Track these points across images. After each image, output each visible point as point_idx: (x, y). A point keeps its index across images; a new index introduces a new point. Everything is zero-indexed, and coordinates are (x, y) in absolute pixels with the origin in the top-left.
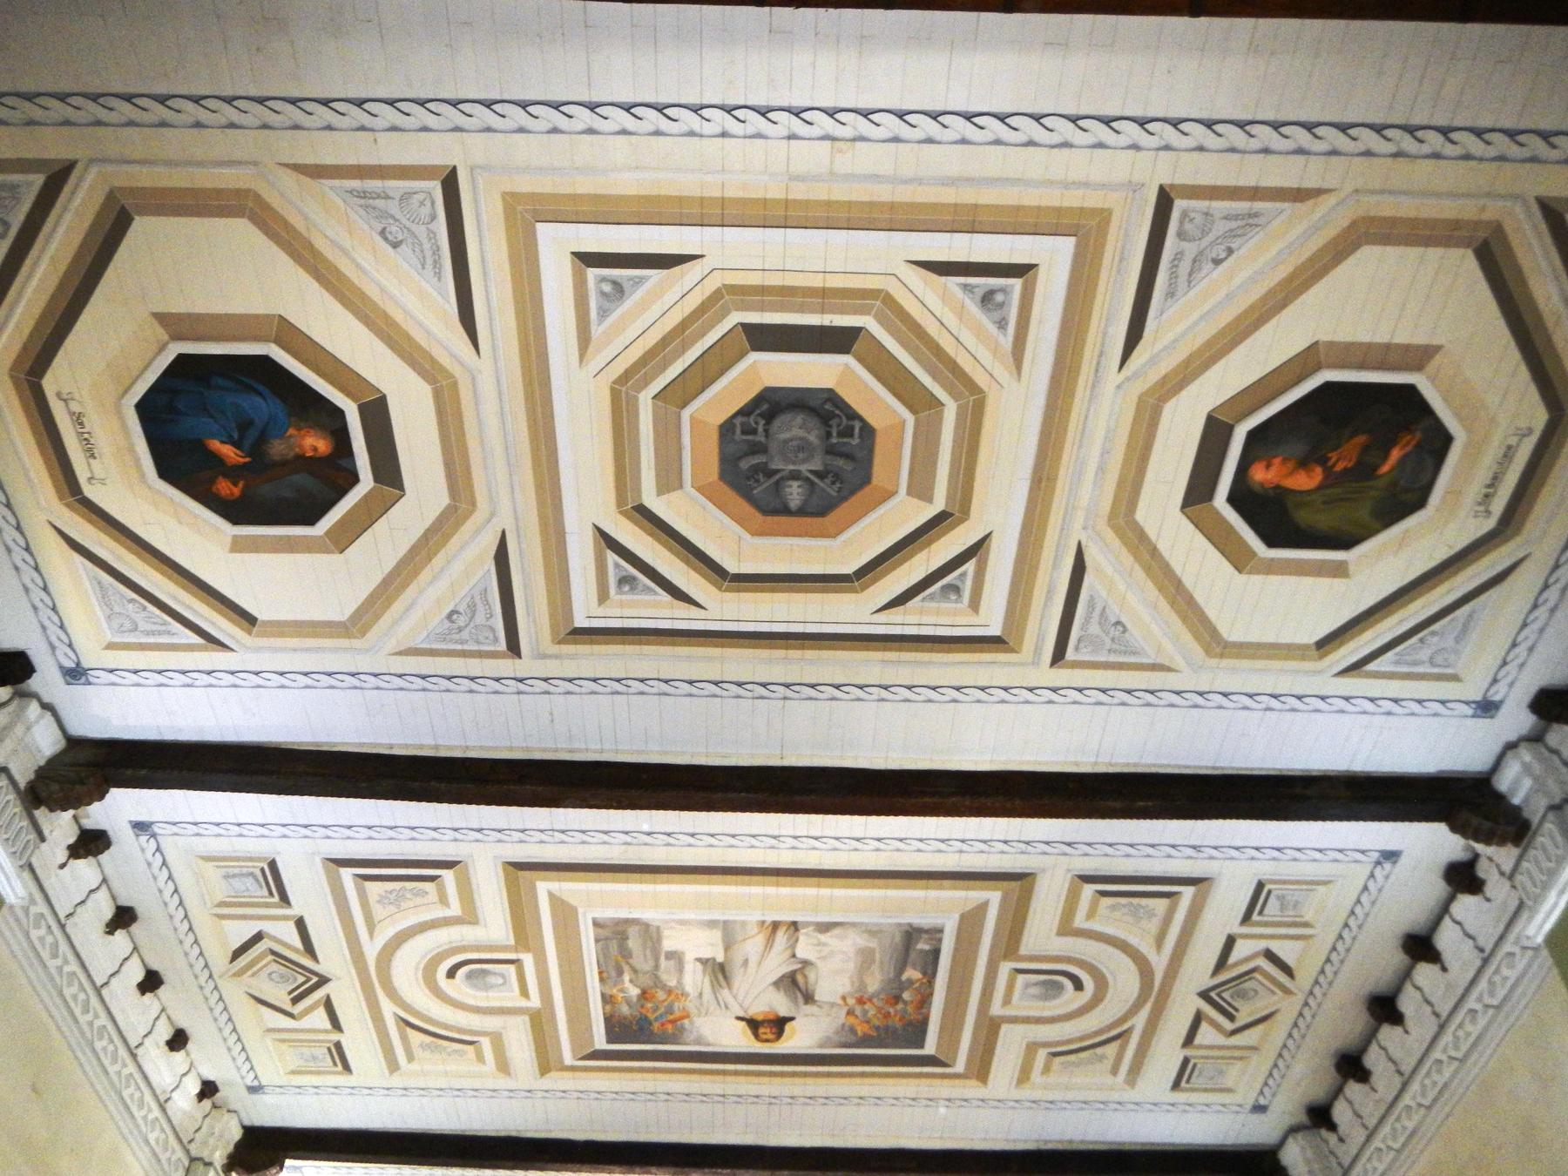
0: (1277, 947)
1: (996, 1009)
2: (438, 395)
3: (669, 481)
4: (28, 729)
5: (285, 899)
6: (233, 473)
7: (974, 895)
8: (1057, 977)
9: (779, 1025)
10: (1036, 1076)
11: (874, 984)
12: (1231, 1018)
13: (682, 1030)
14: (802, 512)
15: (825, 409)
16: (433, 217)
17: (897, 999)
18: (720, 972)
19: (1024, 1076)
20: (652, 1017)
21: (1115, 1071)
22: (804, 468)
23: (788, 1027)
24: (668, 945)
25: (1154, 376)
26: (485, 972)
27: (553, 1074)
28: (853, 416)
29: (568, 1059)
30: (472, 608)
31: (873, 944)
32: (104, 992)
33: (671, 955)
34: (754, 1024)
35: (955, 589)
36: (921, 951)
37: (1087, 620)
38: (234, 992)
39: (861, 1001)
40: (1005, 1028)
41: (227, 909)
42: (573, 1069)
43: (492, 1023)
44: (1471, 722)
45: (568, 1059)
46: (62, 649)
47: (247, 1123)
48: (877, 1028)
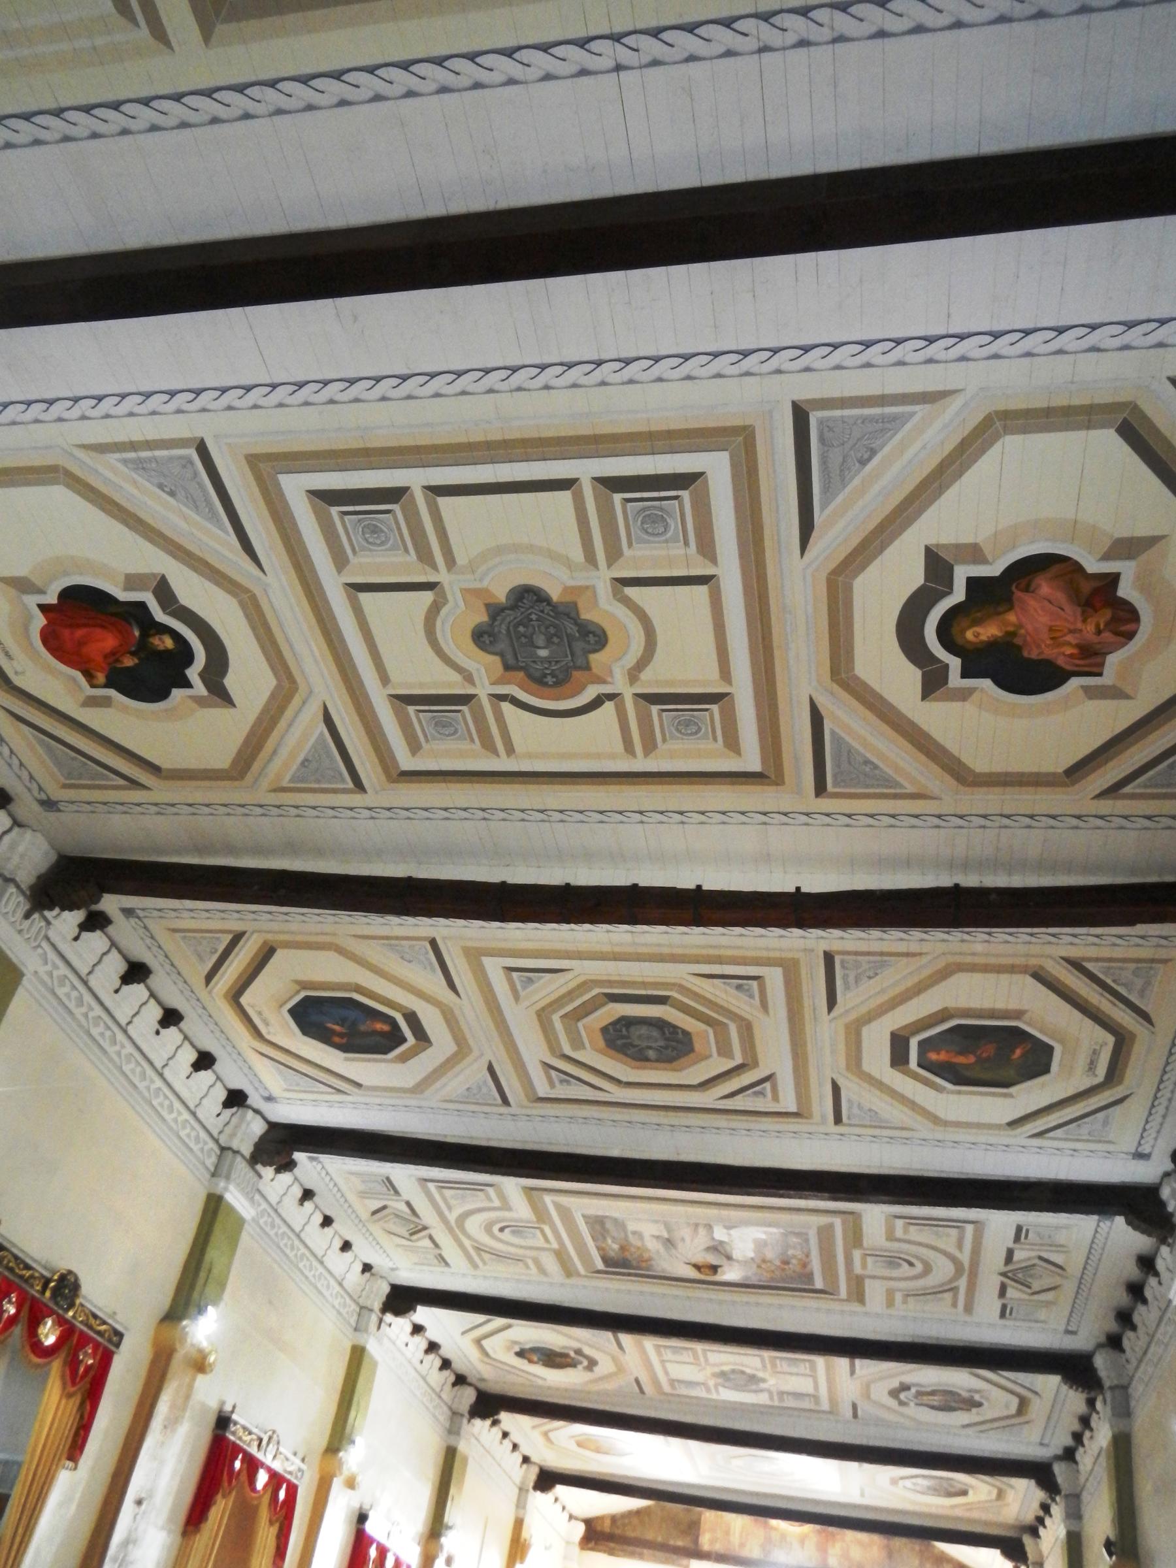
0: (1045, 1255)
1: (858, 1269)
2: (443, 1013)
4: (248, 1124)
5: (397, 1192)
6: (341, 1035)
8: (893, 1261)
9: (714, 1269)
12: (1029, 1287)
14: (657, 1061)
15: (660, 1024)
16: (427, 953)
22: (654, 1045)
25: (853, 1016)
28: (675, 1027)
30: (480, 1088)
32: (303, 1235)
33: (634, 1233)
35: (762, 1093)
37: (850, 1108)
38: (376, 1229)
41: (363, 1195)
43: (534, 1253)
44: (1135, 1162)
46: (261, 1091)
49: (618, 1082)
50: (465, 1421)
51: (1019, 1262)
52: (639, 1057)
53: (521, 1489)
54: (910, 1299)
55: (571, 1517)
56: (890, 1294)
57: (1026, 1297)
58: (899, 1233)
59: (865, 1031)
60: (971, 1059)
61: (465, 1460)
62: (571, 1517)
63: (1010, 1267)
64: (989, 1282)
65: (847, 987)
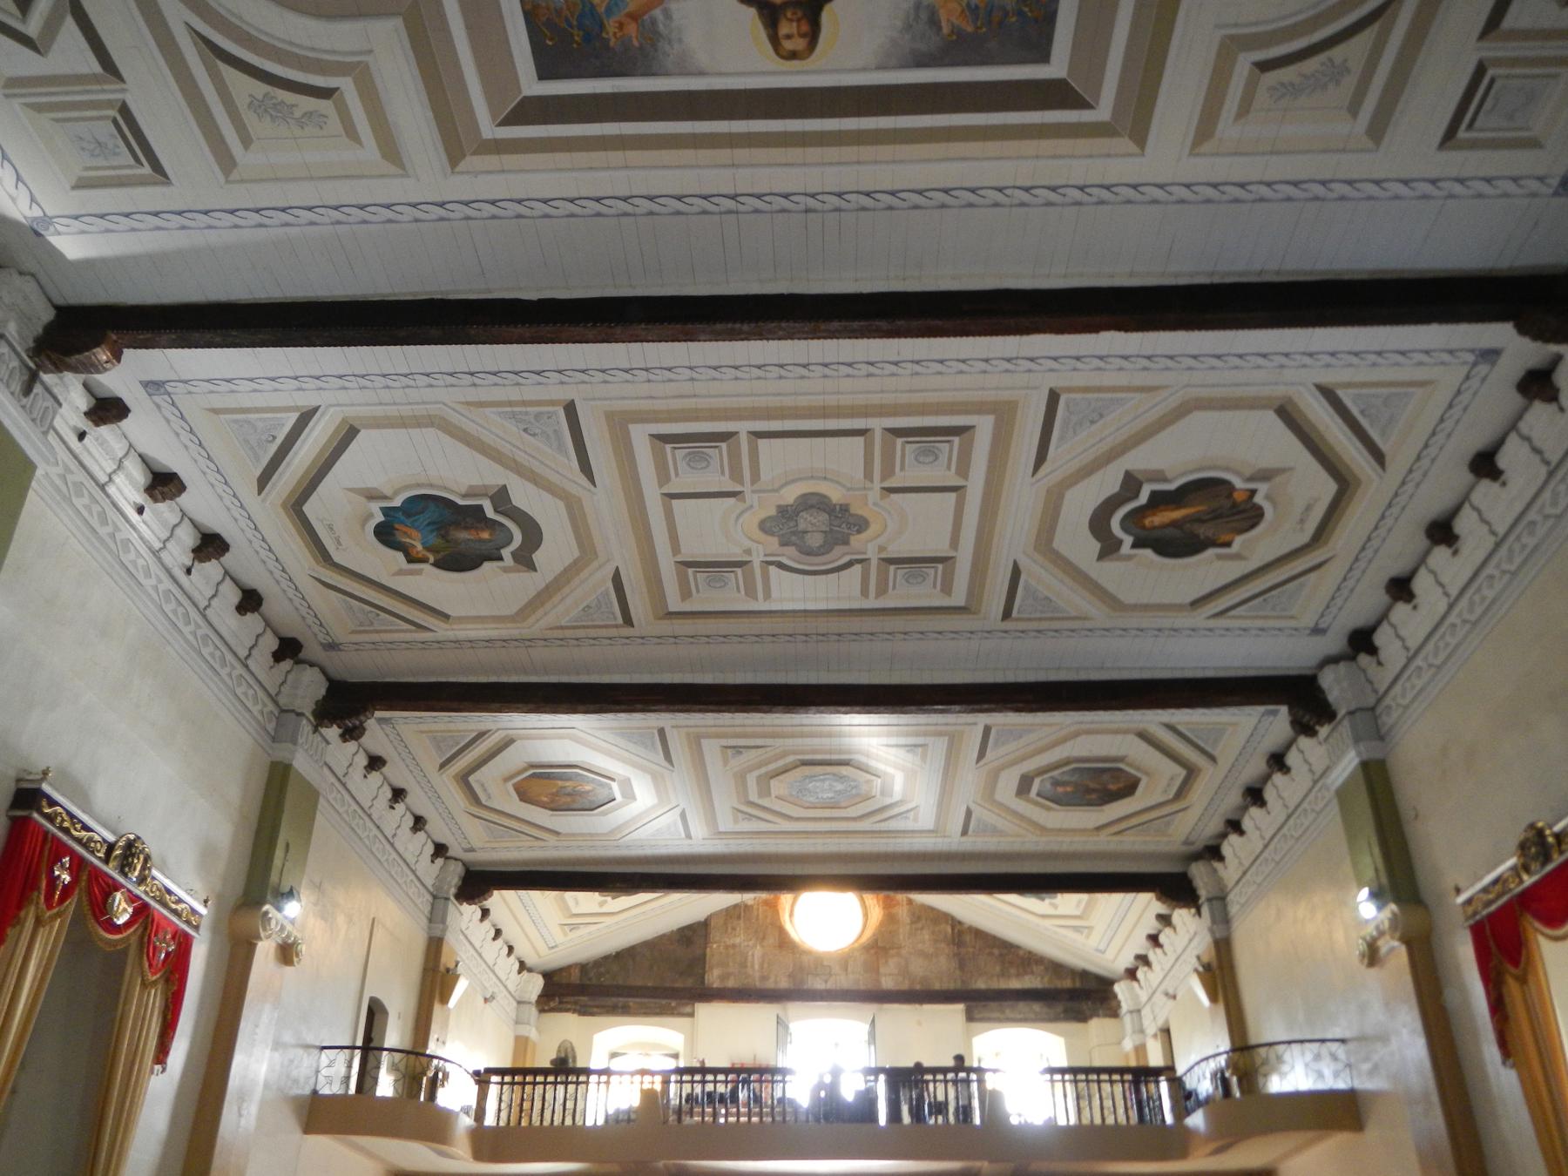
10: (1227, 128)
13: (652, 37)
19: (1205, 129)
21: (1354, 109)
27: (471, 162)
42: (499, 147)
45: (489, 129)
47: (60, 301)
50: (306, 727)
53: (435, 897)
55: (523, 967)
61: (311, 796)
62: (523, 967)
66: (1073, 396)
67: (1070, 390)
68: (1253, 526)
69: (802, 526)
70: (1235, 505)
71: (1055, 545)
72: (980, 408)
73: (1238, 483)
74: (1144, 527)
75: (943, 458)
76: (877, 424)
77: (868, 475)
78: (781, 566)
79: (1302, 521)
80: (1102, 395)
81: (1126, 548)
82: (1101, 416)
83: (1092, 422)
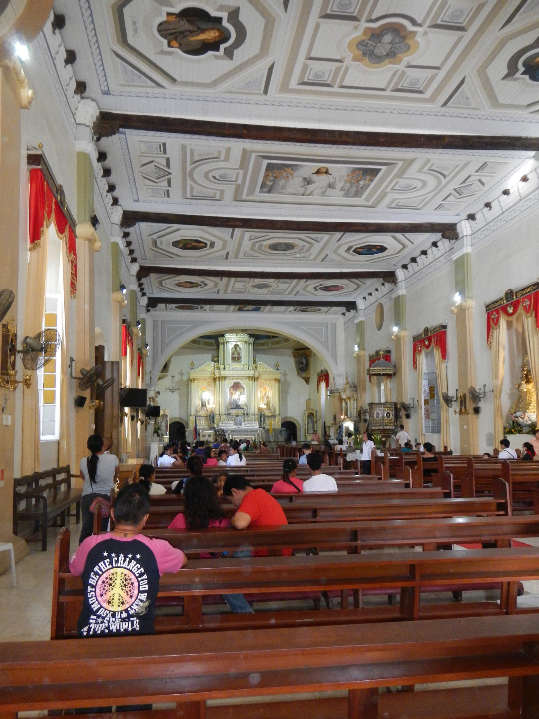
1: (241, 172)
3: (303, 247)
7: (250, 198)
8: (223, 179)
11: (282, 182)
12: (155, 166)
17: (275, 177)
18: (331, 186)
20: (361, 176)
23: (315, 171)
24: (343, 192)
26: (405, 188)
29: (401, 163)
31: (281, 190)
34: (327, 172)
36: (266, 188)
39: (288, 177)
40: (238, 167)
48: (284, 170)
49: (299, 239)
51: (164, 180)
52: (286, 244)
54: (216, 156)
56: (227, 159)
57: (155, 159)
58: (218, 193)
59: (221, 248)
60: (193, 244)
63: (168, 176)
64: (175, 168)
65: (224, 256)
66: (258, 92)
67: (260, 94)
68: (161, 24)
69: (390, 46)
70: (176, 39)
71: (264, 21)
72: (294, 91)
73: (178, 51)
74: (219, 30)
75: (312, 73)
76: (336, 89)
77: (347, 69)
78: (414, 22)
79: (134, 23)
80: (247, 91)
81: (224, 15)
82: (246, 84)
83: (250, 82)
